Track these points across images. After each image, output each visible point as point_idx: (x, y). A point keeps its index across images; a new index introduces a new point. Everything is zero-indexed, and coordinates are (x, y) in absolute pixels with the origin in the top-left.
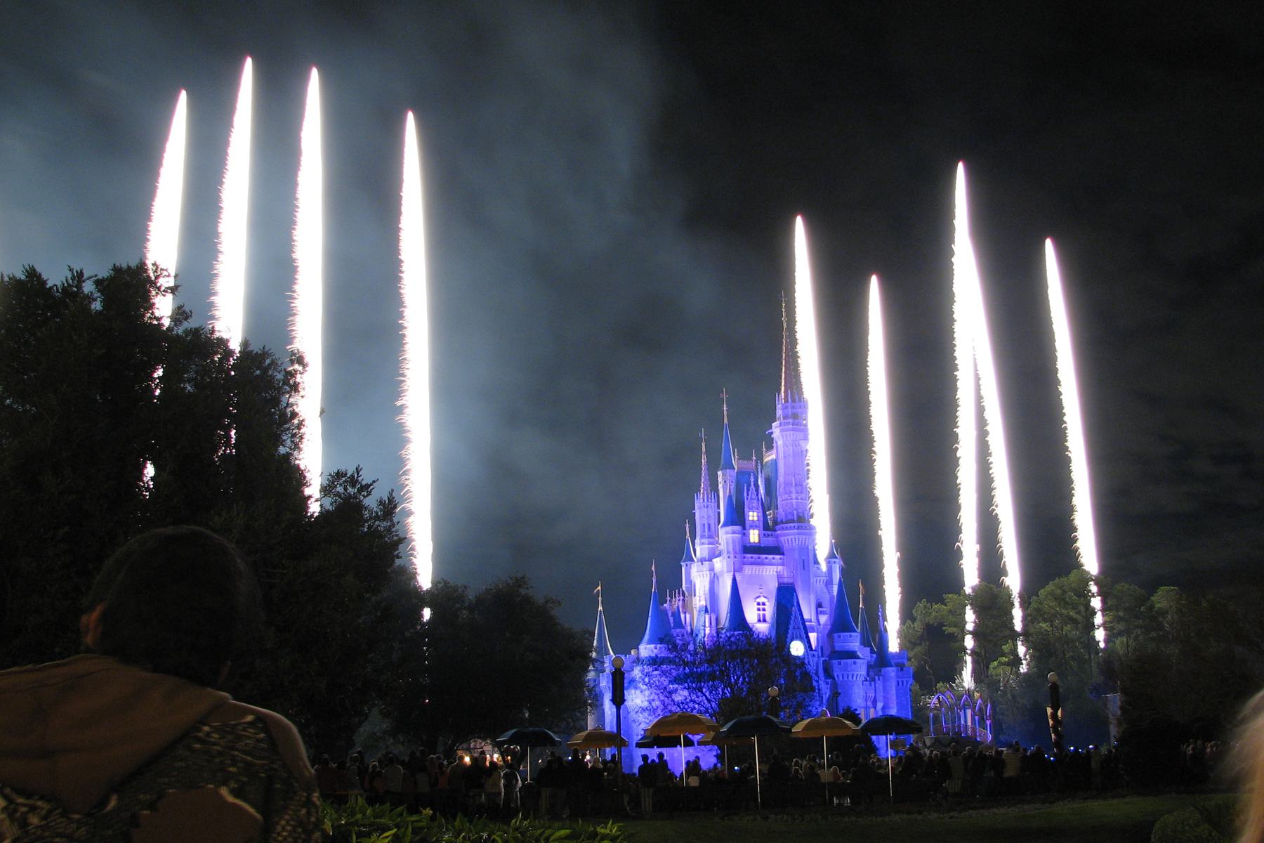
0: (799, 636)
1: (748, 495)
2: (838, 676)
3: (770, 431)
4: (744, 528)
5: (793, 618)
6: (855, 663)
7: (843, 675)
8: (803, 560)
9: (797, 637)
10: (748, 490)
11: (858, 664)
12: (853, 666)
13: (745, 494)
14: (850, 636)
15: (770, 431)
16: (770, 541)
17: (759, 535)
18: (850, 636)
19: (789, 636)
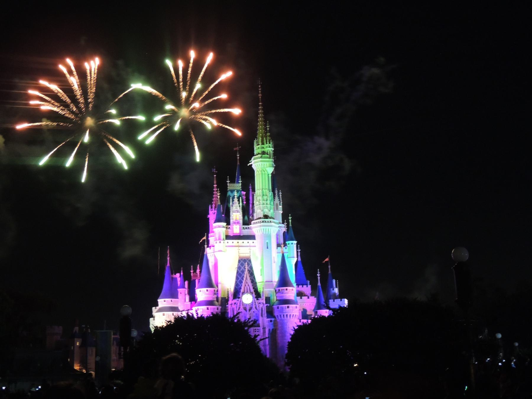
0: (249, 291)
1: (233, 203)
2: (277, 316)
3: (250, 164)
4: (228, 223)
5: (244, 279)
6: (288, 307)
7: (280, 315)
8: (267, 243)
9: (247, 292)
10: (233, 201)
11: (290, 308)
12: (287, 309)
13: (231, 203)
14: (286, 290)
15: (250, 164)
16: (246, 232)
17: (240, 228)
18: (286, 290)
19: (242, 290)
